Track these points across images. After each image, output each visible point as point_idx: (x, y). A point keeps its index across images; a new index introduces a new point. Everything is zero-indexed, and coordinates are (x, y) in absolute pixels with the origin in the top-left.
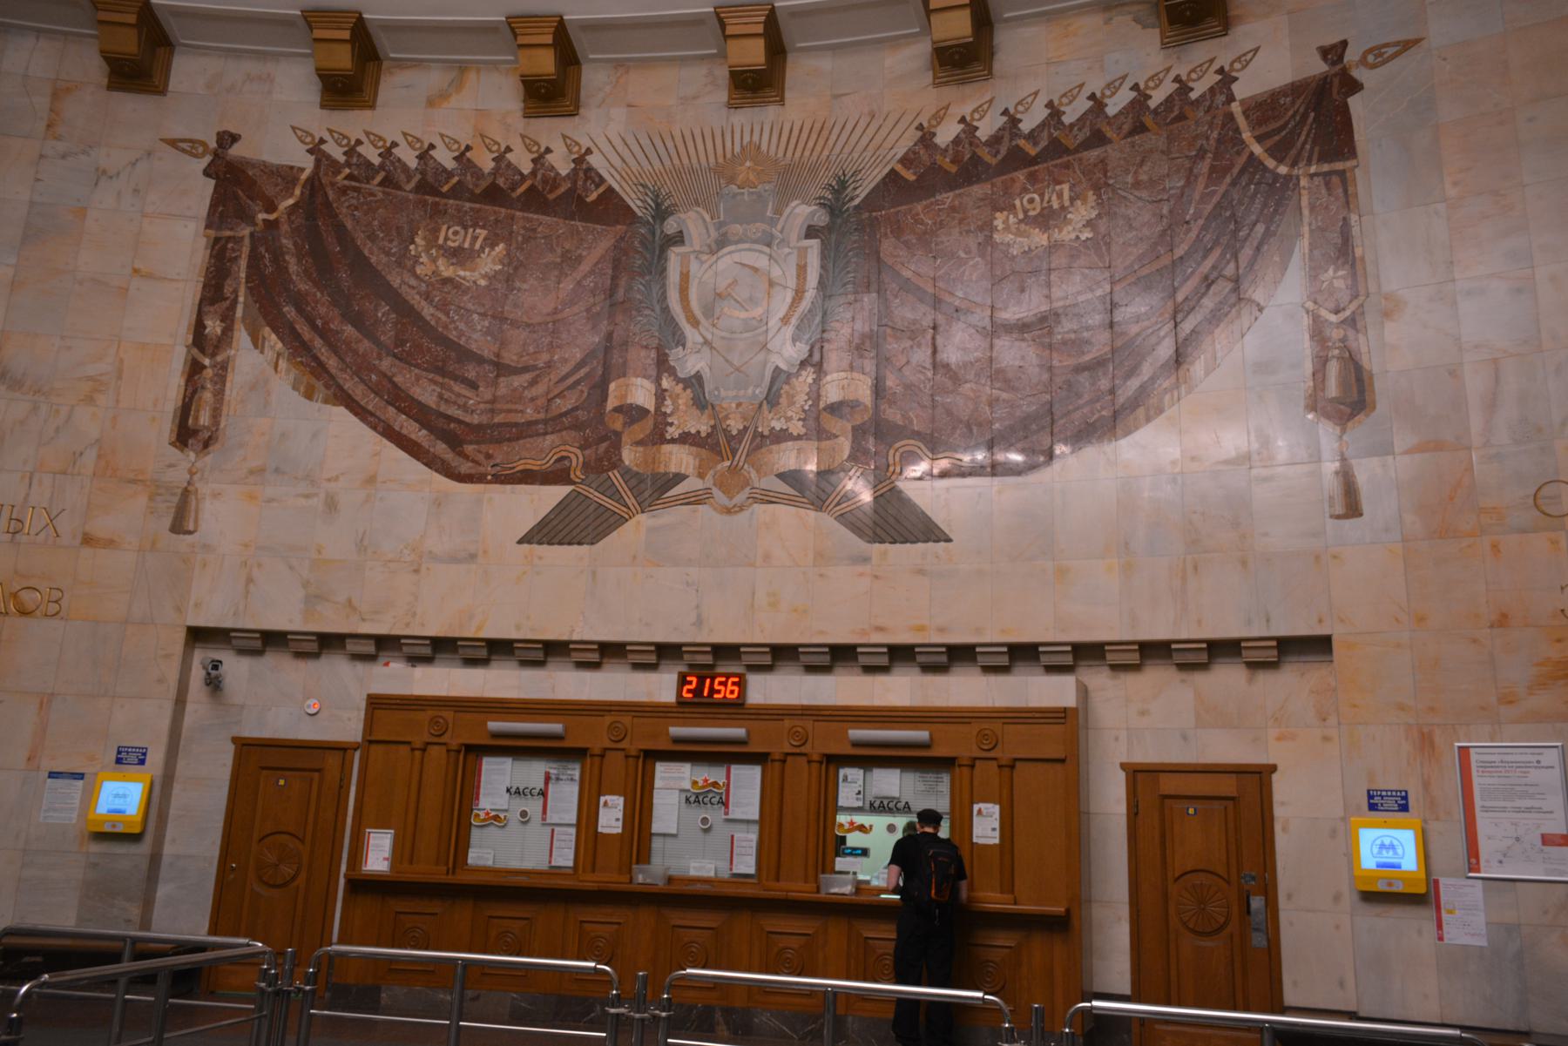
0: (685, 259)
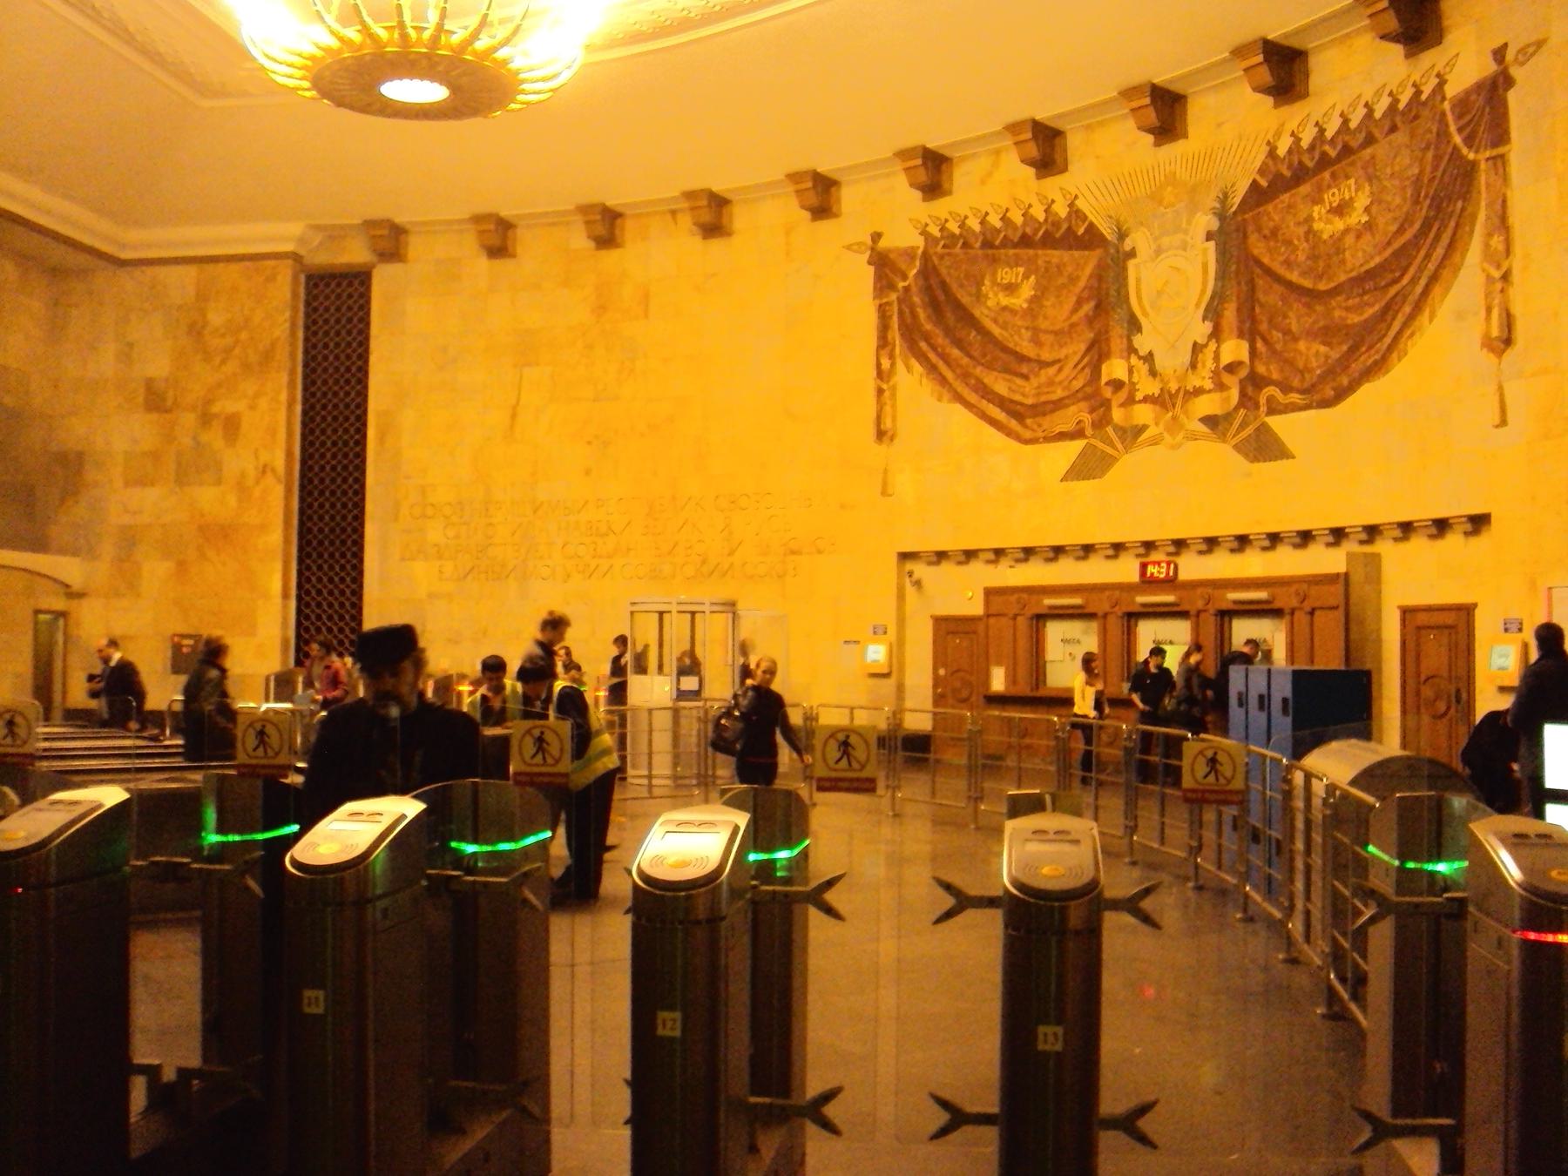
0: (1137, 266)
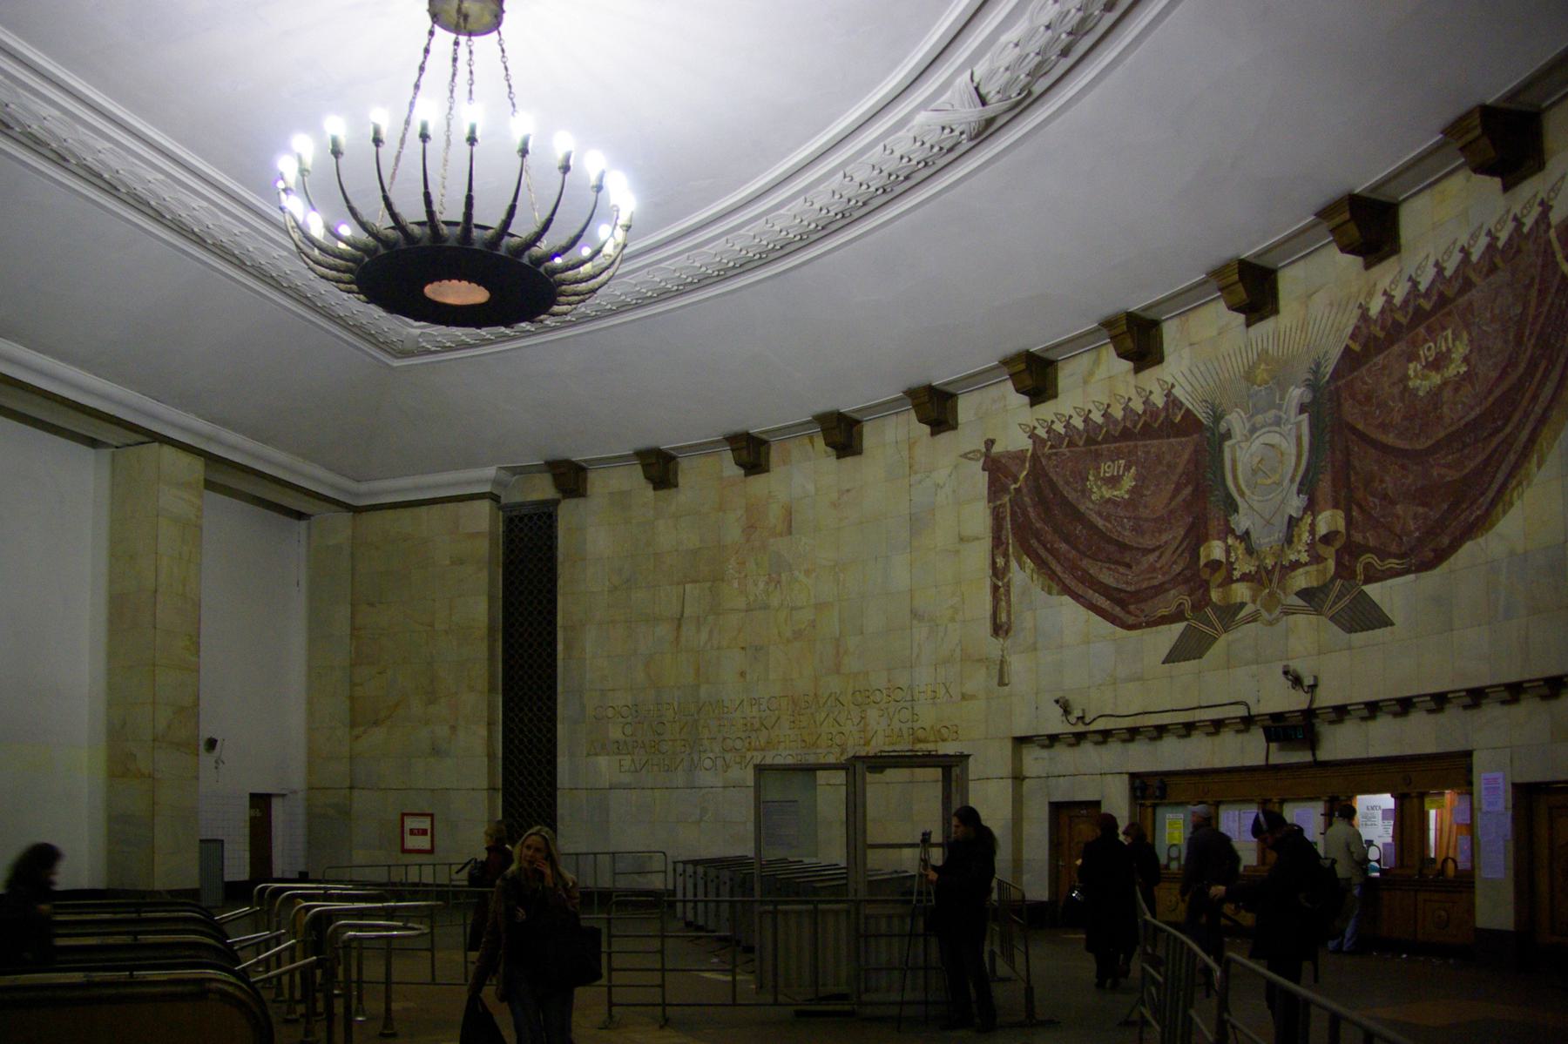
0: (1232, 448)
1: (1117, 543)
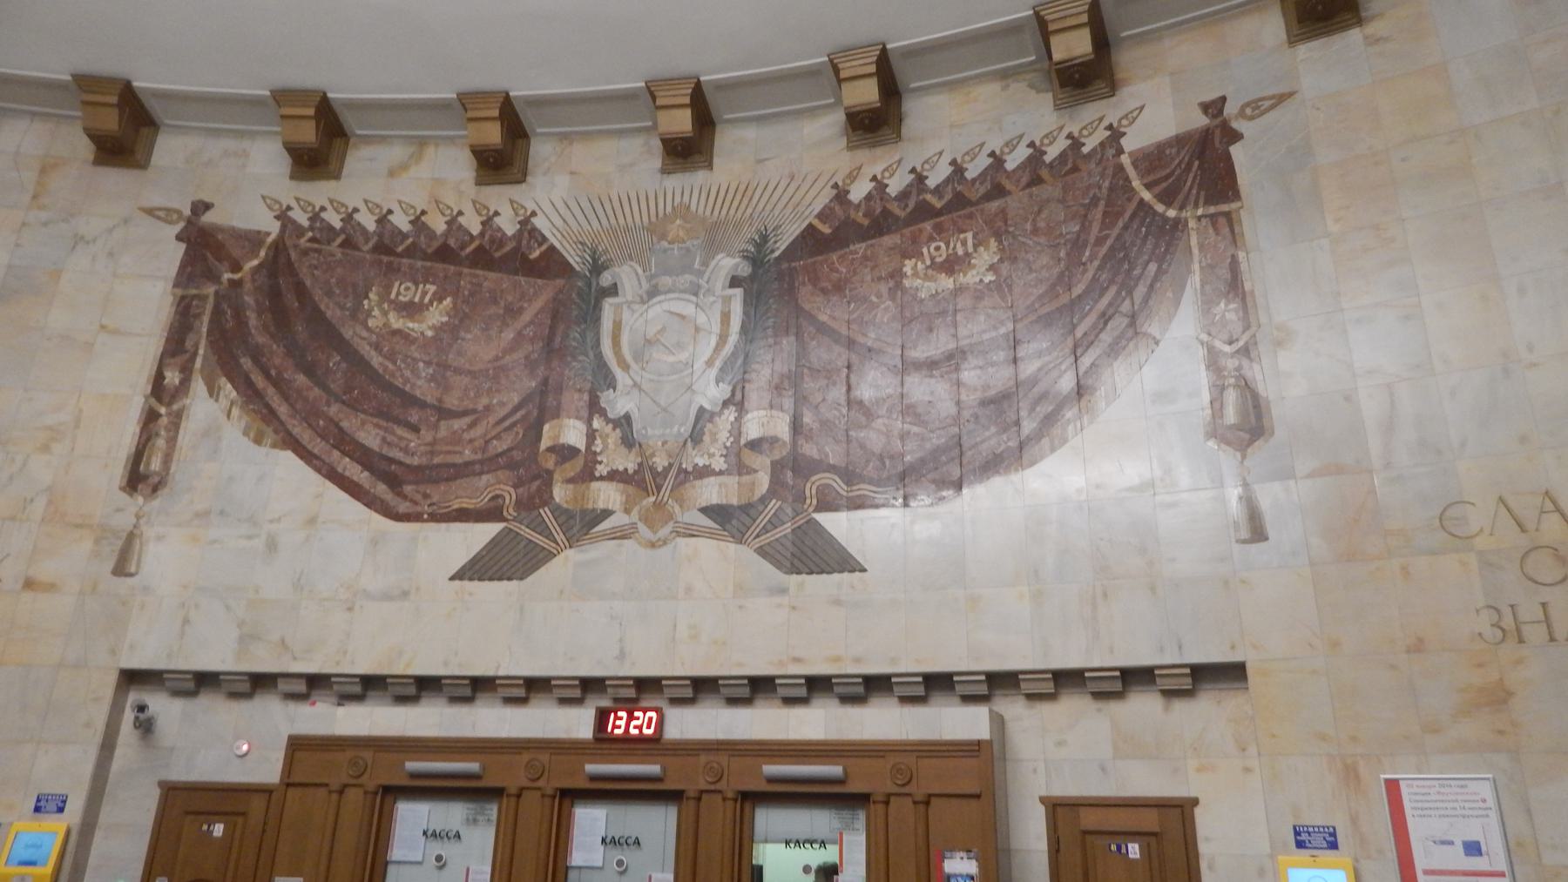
0: (618, 307)
1: (401, 393)
